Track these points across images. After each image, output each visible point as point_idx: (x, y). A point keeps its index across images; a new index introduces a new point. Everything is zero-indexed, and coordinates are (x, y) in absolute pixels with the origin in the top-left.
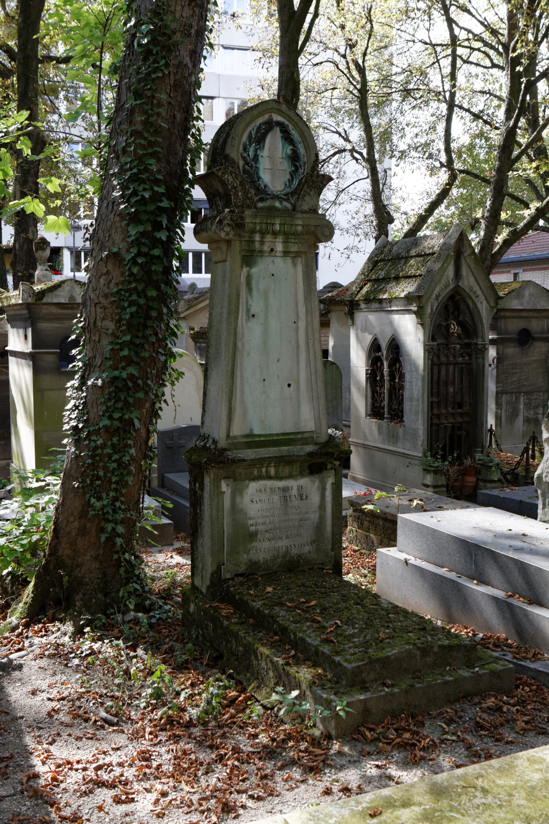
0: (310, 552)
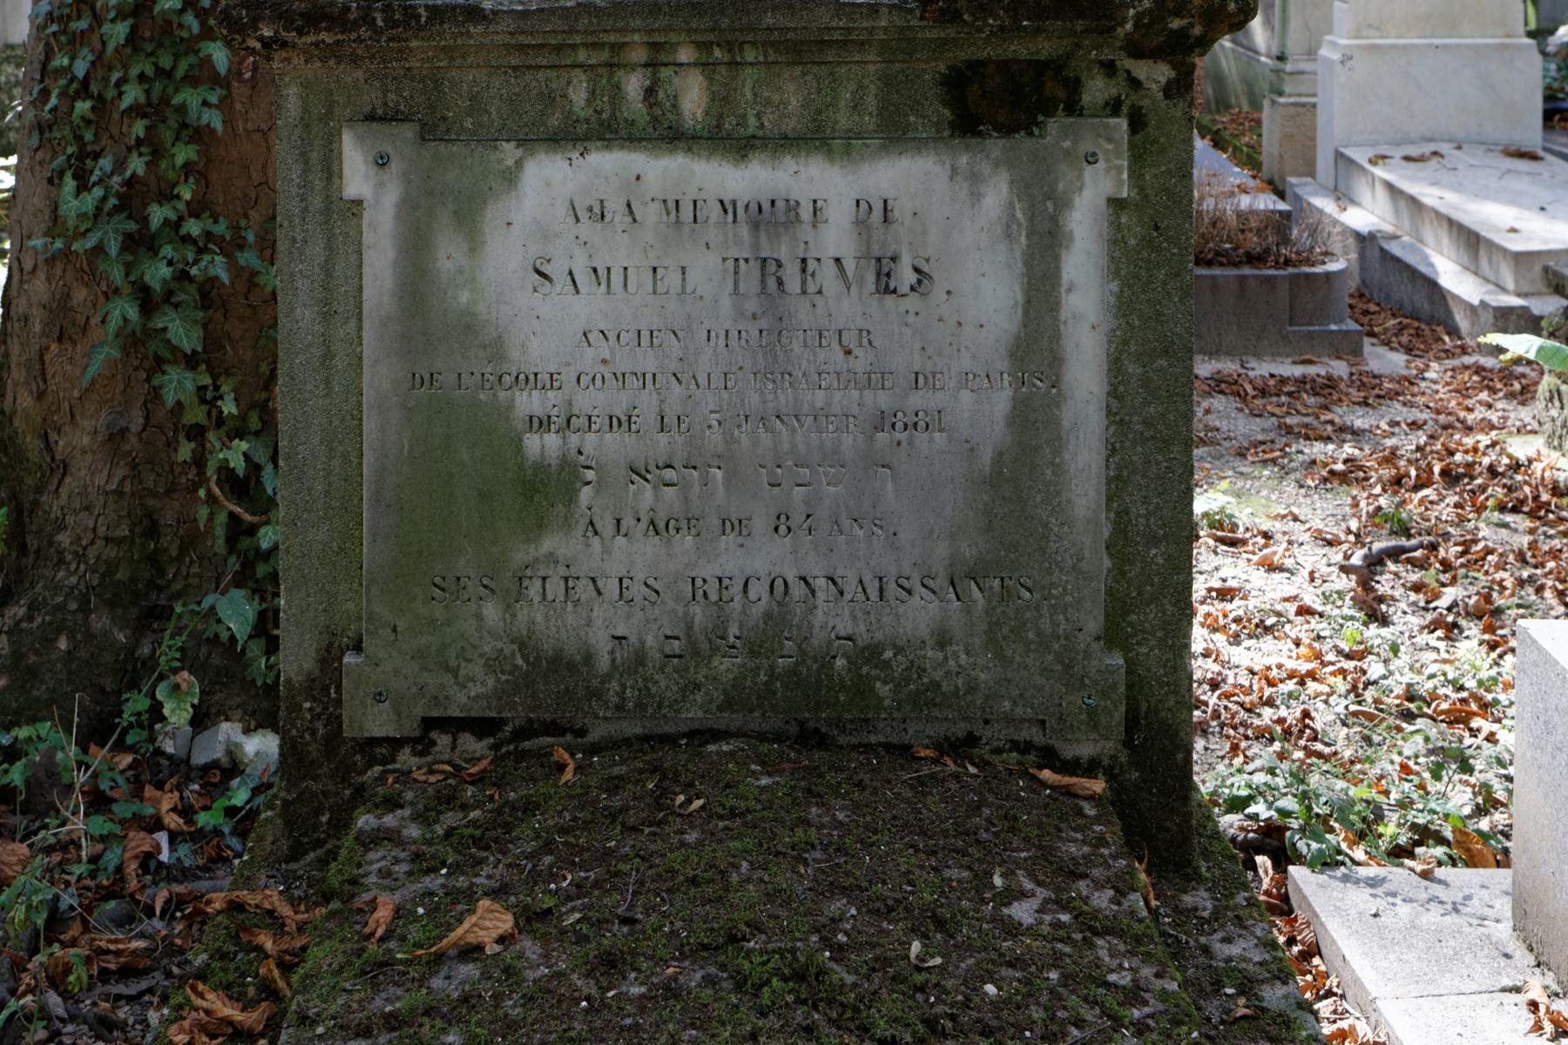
0: (943, 641)
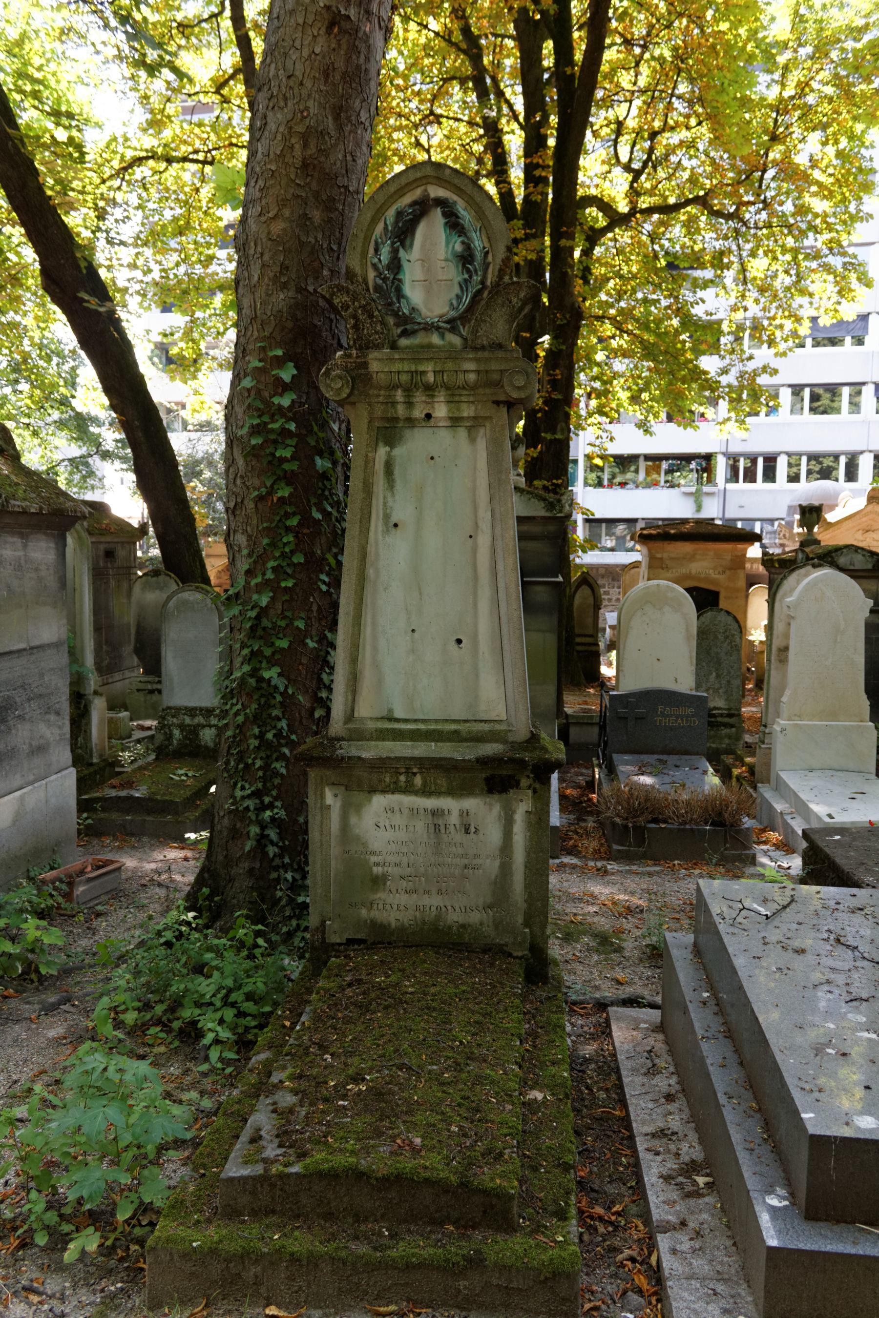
0: (481, 924)
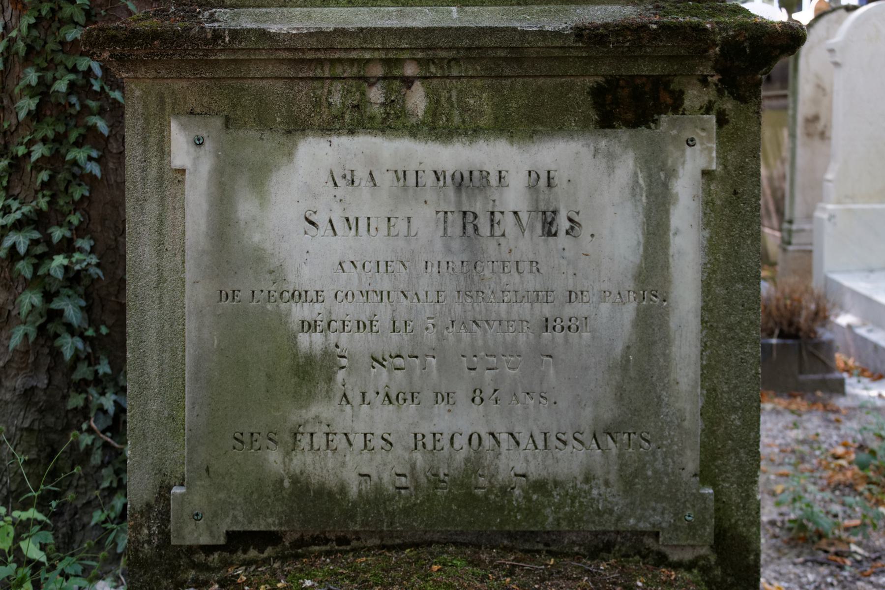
0: (588, 479)
